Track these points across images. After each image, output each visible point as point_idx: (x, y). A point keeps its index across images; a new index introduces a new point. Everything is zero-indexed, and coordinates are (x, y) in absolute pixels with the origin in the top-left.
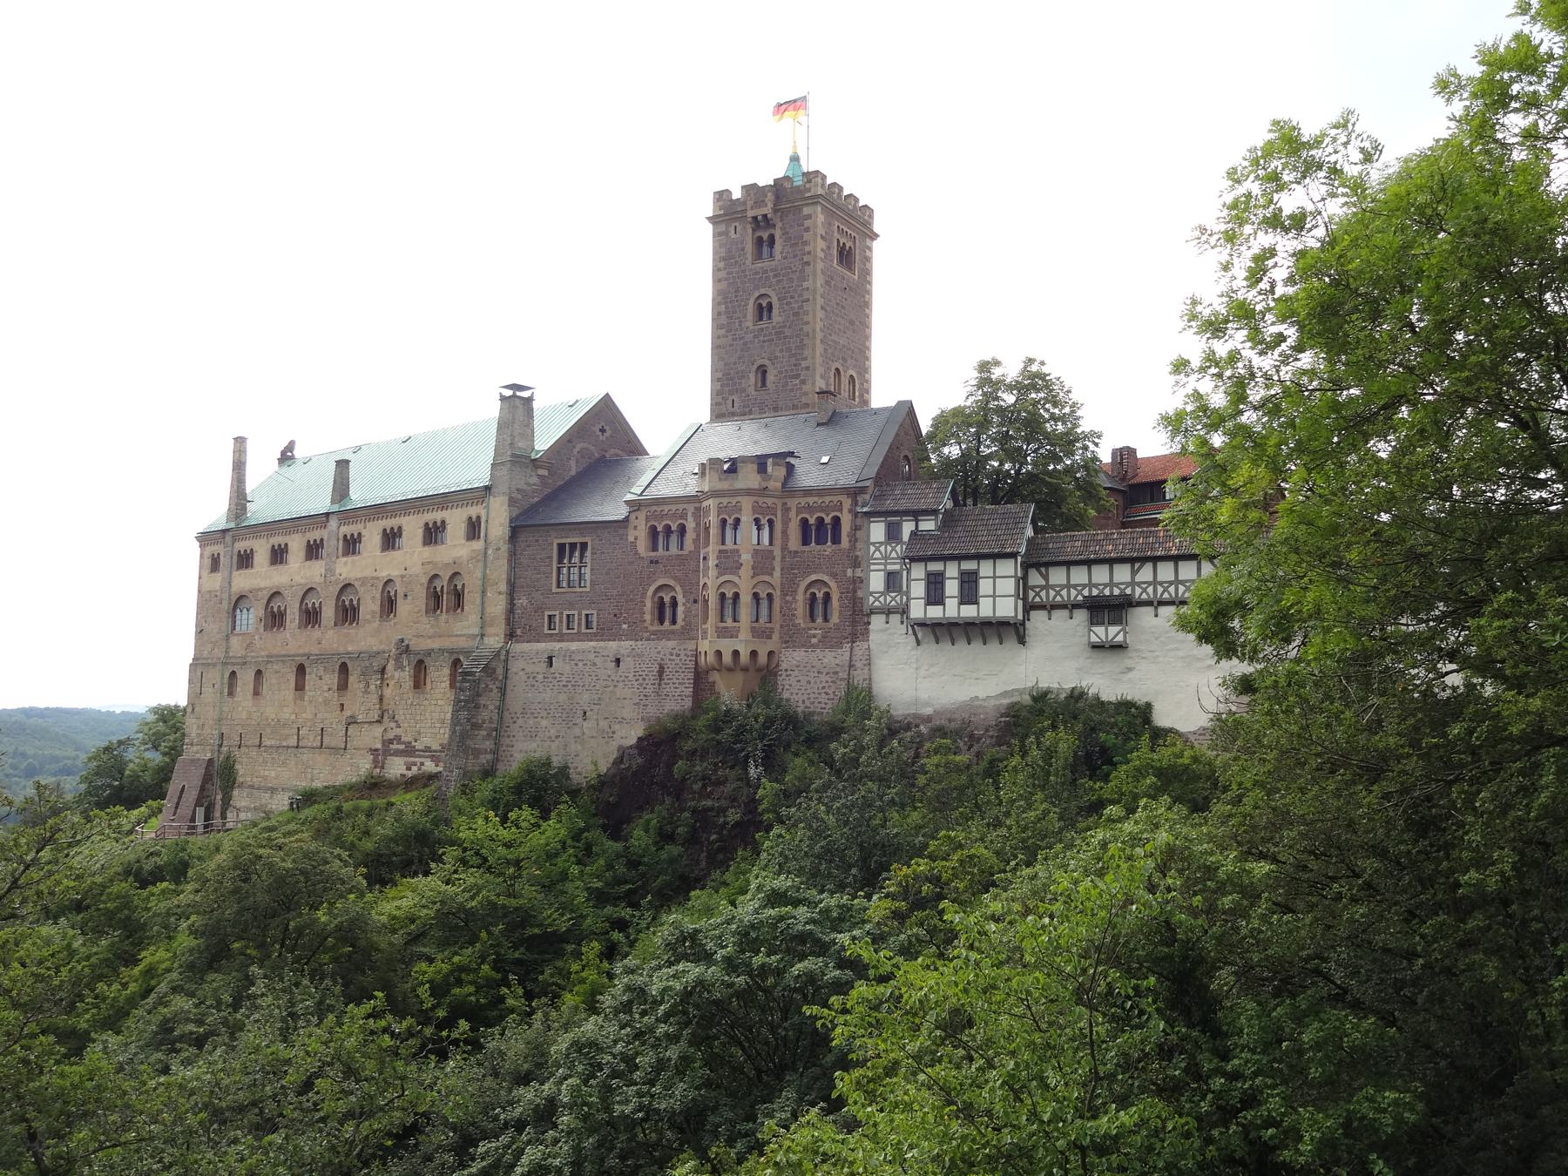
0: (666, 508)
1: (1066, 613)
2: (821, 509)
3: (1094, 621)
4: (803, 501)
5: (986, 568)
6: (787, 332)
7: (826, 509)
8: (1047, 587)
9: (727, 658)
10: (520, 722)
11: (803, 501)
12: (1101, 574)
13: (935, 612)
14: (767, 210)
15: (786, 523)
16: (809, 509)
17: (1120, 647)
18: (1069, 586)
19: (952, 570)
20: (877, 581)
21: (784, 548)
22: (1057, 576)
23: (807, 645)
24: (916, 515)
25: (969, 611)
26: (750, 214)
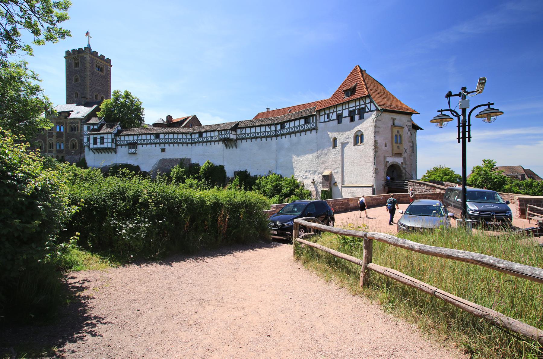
1: (124, 147)
2: (74, 123)
3: (130, 148)
5: (105, 136)
8: (120, 141)
12: (131, 138)
13: (95, 146)
14: (76, 56)
16: (72, 123)
17: (135, 154)
18: (125, 140)
19: (99, 136)
20: (85, 140)
21: (66, 132)
22: (122, 138)
25: (102, 146)
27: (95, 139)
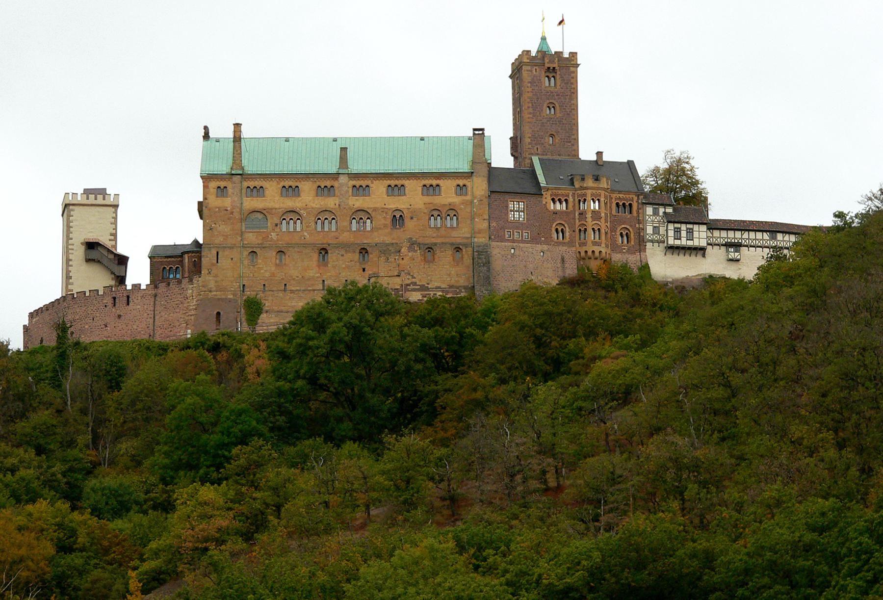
0: (560, 192)
4: (618, 196)
5: (696, 227)
6: (564, 121)
7: (627, 200)
9: (597, 254)
10: (502, 275)
11: (618, 196)
12: (731, 234)
13: (678, 242)
15: (611, 203)
17: (738, 260)
19: (684, 227)
20: (650, 230)
23: (621, 252)
24: (665, 205)
25: (690, 243)
26: (547, 65)
27: (677, 231)
